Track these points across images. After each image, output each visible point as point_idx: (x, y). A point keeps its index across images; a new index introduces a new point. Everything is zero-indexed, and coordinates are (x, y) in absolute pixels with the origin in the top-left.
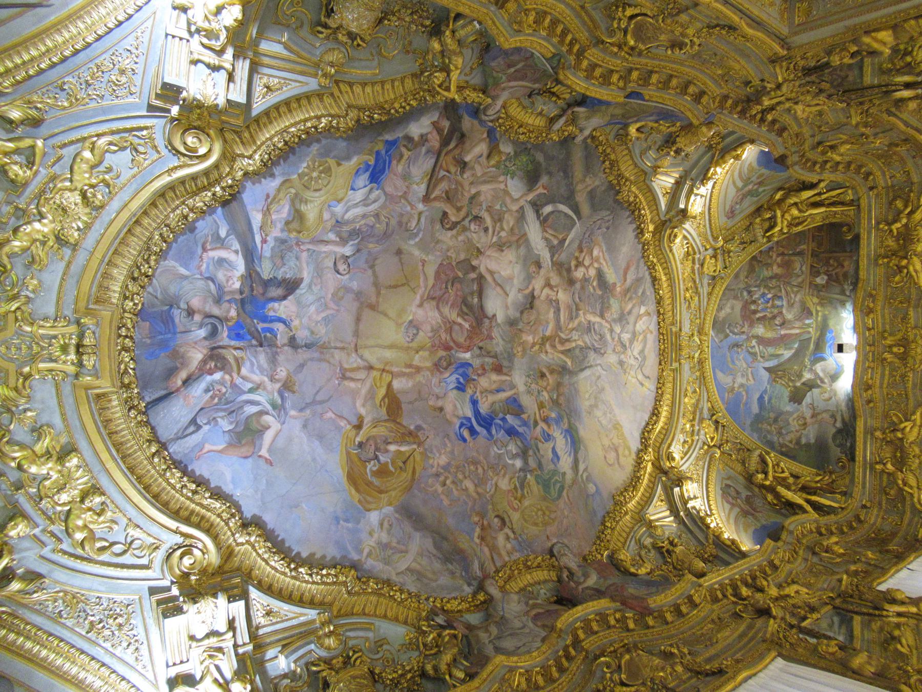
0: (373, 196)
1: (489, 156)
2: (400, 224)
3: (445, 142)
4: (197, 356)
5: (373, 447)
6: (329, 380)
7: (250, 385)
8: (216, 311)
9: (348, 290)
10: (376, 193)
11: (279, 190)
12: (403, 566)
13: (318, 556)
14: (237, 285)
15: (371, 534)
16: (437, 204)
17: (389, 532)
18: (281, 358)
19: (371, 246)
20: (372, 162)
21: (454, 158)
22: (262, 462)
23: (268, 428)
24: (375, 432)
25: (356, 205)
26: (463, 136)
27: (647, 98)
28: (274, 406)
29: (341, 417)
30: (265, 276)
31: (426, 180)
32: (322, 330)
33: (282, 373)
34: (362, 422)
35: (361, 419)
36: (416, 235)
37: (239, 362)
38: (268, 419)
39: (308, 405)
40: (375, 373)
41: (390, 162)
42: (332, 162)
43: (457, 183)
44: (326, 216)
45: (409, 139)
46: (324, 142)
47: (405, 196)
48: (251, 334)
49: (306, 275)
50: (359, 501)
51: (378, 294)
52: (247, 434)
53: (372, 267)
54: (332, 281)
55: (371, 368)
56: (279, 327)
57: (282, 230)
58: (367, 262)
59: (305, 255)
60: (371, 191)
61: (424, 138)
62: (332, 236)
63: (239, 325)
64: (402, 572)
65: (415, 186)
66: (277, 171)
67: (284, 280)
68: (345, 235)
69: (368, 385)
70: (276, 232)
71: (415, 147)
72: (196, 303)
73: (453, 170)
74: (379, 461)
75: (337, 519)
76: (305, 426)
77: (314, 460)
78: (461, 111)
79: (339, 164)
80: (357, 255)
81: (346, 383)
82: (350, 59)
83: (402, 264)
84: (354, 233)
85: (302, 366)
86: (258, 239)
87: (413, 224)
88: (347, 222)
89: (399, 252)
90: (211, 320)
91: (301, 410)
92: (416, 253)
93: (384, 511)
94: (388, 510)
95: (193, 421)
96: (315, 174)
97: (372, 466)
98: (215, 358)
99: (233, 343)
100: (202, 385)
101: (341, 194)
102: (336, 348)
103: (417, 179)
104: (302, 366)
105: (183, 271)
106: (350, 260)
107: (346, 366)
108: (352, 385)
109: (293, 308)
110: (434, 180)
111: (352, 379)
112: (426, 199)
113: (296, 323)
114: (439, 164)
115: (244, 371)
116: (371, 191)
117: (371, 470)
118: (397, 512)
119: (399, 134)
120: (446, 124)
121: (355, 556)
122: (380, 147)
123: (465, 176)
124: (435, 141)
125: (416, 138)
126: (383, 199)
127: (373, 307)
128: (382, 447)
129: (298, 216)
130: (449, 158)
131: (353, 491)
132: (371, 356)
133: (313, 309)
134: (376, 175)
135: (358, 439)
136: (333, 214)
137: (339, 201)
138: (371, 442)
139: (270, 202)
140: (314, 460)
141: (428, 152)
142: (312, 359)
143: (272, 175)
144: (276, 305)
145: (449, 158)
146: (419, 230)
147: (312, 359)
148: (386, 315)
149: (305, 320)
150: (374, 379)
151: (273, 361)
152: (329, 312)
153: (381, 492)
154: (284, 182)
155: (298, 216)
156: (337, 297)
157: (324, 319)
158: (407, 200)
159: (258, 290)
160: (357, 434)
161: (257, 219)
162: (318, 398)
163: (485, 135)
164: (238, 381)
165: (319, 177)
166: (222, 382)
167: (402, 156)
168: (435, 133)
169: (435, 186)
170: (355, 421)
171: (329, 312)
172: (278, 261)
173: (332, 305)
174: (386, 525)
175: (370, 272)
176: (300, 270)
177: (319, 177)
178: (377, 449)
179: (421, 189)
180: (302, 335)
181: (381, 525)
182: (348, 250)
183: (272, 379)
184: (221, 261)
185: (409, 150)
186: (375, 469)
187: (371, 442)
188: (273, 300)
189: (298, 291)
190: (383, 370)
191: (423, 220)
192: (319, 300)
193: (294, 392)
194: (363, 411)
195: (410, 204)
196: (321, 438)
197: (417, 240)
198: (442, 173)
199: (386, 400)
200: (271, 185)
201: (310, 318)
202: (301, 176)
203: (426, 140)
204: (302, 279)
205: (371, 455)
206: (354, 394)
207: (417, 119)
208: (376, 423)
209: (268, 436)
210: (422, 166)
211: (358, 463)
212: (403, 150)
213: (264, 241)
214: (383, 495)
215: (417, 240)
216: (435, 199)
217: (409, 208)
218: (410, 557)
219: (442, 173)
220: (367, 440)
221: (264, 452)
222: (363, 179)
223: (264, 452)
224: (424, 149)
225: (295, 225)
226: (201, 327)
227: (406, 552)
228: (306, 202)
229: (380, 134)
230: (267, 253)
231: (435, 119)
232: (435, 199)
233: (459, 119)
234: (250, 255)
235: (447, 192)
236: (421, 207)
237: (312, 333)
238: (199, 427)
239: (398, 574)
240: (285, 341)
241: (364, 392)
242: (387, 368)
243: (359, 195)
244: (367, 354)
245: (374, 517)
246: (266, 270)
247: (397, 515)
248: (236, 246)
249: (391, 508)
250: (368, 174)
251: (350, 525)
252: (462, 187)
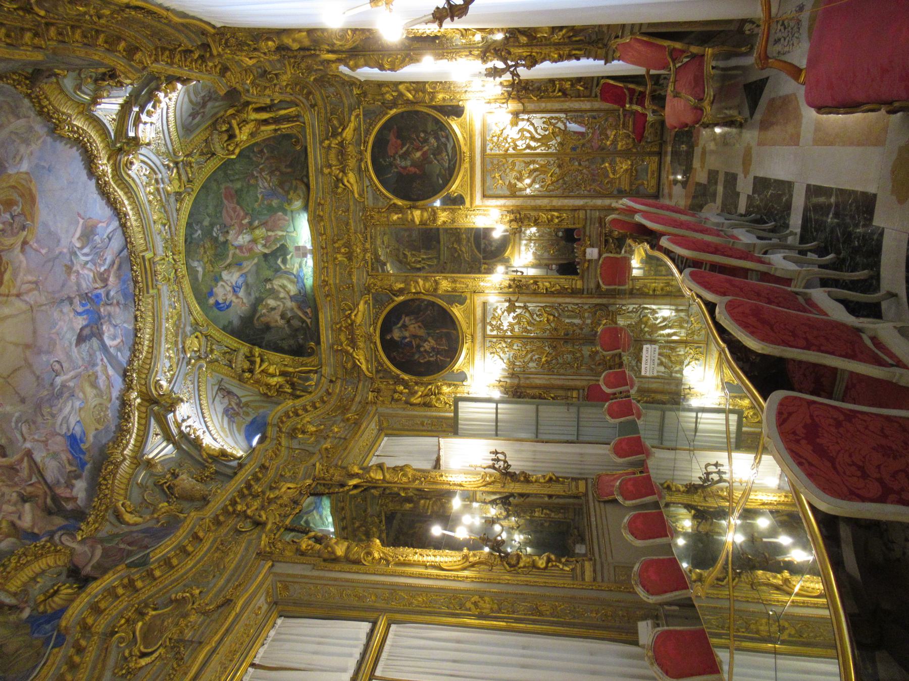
0: (65, 426)
1: (13, 524)
2: (34, 423)
3: (55, 499)
4: (112, 280)
5: (15, 226)
6: (46, 279)
7: (88, 266)
8: (109, 308)
9: (48, 352)
10: (64, 431)
11: (110, 393)
12: (22, 122)
13: (69, 146)
14: (104, 327)
15: (32, 153)
16: (16, 457)
17: (18, 151)
18: (75, 288)
19: (46, 393)
20: (82, 445)
21: (37, 496)
22: (82, 214)
23: (79, 239)
24: (11, 240)
25: (70, 413)
26: (50, 513)
27: (56, 650)
28: (75, 254)
29: (36, 250)
30: (94, 340)
31: (41, 466)
32: (56, 315)
33: (73, 277)
34: (22, 248)
35: (23, 250)
36: (17, 422)
37: (95, 281)
38: (78, 245)
39: (57, 257)
40: (14, 291)
41: (73, 455)
42: (100, 427)
43: (16, 485)
44: (81, 395)
45: (78, 477)
46: (112, 434)
47: (45, 442)
48: (92, 300)
49: (74, 350)
50: (31, 182)
51: (26, 360)
52: (88, 234)
53: (38, 378)
54: (60, 355)
55: (18, 295)
56: (80, 309)
57: (97, 372)
58: (43, 379)
59: (80, 363)
60: (68, 429)
61: (71, 486)
62: (71, 384)
63: (97, 303)
64: (25, 117)
65: (44, 454)
66: (117, 403)
67: (84, 341)
68: (65, 389)
69: (19, 280)
70: (99, 368)
71: (68, 477)
72: (117, 309)
73: (29, 489)
74: (11, 215)
75: (49, 170)
76: (59, 241)
77: (55, 216)
78: (72, 521)
79: (96, 429)
80: (51, 381)
81: (34, 279)
82: (152, 475)
83: (17, 393)
84: (60, 395)
85: (63, 286)
86: (105, 360)
87: (25, 429)
88: (68, 399)
89: (23, 401)
90: (109, 302)
91: (60, 253)
92: (8, 408)
93: (15, 171)
94: (11, 171)
95: (110, 239)
96: (102, 414)
97: (17, 210)
98: (103, 278)
99: (99, 291)
100: (108, 262)
101: (83, 414)
102: (45, 305)
103: (47, 460)
104: (63, 286)
105: (125, 325)
106: (54, 374)
107: (36, 292)
108: (30, 278)
109: (75, 325)
110: (36, 470)
111: (30, 282)
112: (29, 454)
113: (72, 315)
114: (42, 482)
115: (92, 275)
116: (68, 429)
117: (18, 206)
118: (5, 168)
119: (85, 473)
120: (69, 506)
121: (49, 139)
122: (86, 458)
123: (14, 495)
124: (62, 491)
125: (74, 481)
126: (58, 430)
127: (27, 346)
128: (8, 228)
129: (94, 385)
130: (41, 492)
131: (34, 191)
132: (19, 305)
133: (65, 329)
134: (73, 441)
135: (25, 233)
136: (78, 398)
137: (80, 409)
138: (15, 231)
139: (110, 385)
140: (55, 216)
141: (58, 482)
142: (59, 292)
143: (117, 399)
144: (85, 323)
145: (41, 492)
146: (16, 427)
147: (59, 292)
148: (16, 345)
149: (67, 318)
150: (14, 286)
151: (78, 285)
152: (54, 331)
153: (14, 187)
154: (111, 400)
155: (94, 385)
156: (52, 343)
157: (57, 324)
158: (43, 441)
159: (95, 330)
160: (25, 238)
161: (111, 371)
162: (51, 264)
163: (36, 531)
164: (93, 268)
165: (99, 414)
166: (100, 265)
167: (70, 464)
168: (68, 495)
169: (30, 467)
170: (27, 248)
171: (54, 331)
172: (91, 351)
173: (54, 336)
174: (18, 159)
175: (38, 373)
176: (79, 352)
177: (99, 414)
178: (11, 225)
179: (38, 457)
180: (66, 309)
181: (21, 159)
182: (59, 380)
183: (78, 272)
184: (114, 338)
185: (70, 472)
186: (15, 208)
187: (15, 231)
188: (86, 326)
189: (75, 337)
190: (8, 296)
191: (19, 437)
192: (63, 337)
193: (66, 265)
194: (21, 257)
195: (38, 441)
196: (50, 233)
197: (14, 419)
198: (34, 480)
199: (3, 269)
200: (115, 394)
201: (65, 321)
202: (107, 408)
203: (67, 487)
204: (76, 346)
205: (17, 219)
206: (29, 271)
207: (86, 490)
208: (11, 248)
209: (78, 234)
210: (52, 471)
211: (27, 213)
212: (74, 469)
213: (102, 360)
214: (14, 184)
215: (14, 419)
216: (22, 460)
217: (36, 437)
218: (12, 127)
219: (34, 480)
220: (18, 233)
221: (81, 221)
222: (78, 431)
223: (81, 221)
224: (62, 481)
225: (93, 378)
226: (113, 298)
227: (12, 132)
228: (95, 396)
229: (94, 463)
230: (98, 353)
231: (79, 502)
232: (22, 460)
233: (66, 518)
234: (104, 348)
235: (17, 471)
236: (28, 445)
237: (61, 311)
238: (108, 237)
239: (29, 117)
240: (75, 301)
241: (21, 274)
242: (5, 298)
243: (73, 421)
244: (23, 306)
245: (25, 167)
246: (95, 342)
247: (7, 165)
248: (112, 350)
249: (10, 172)
250: (78, 437)
251: (43, 164)
252: (7, 485)
